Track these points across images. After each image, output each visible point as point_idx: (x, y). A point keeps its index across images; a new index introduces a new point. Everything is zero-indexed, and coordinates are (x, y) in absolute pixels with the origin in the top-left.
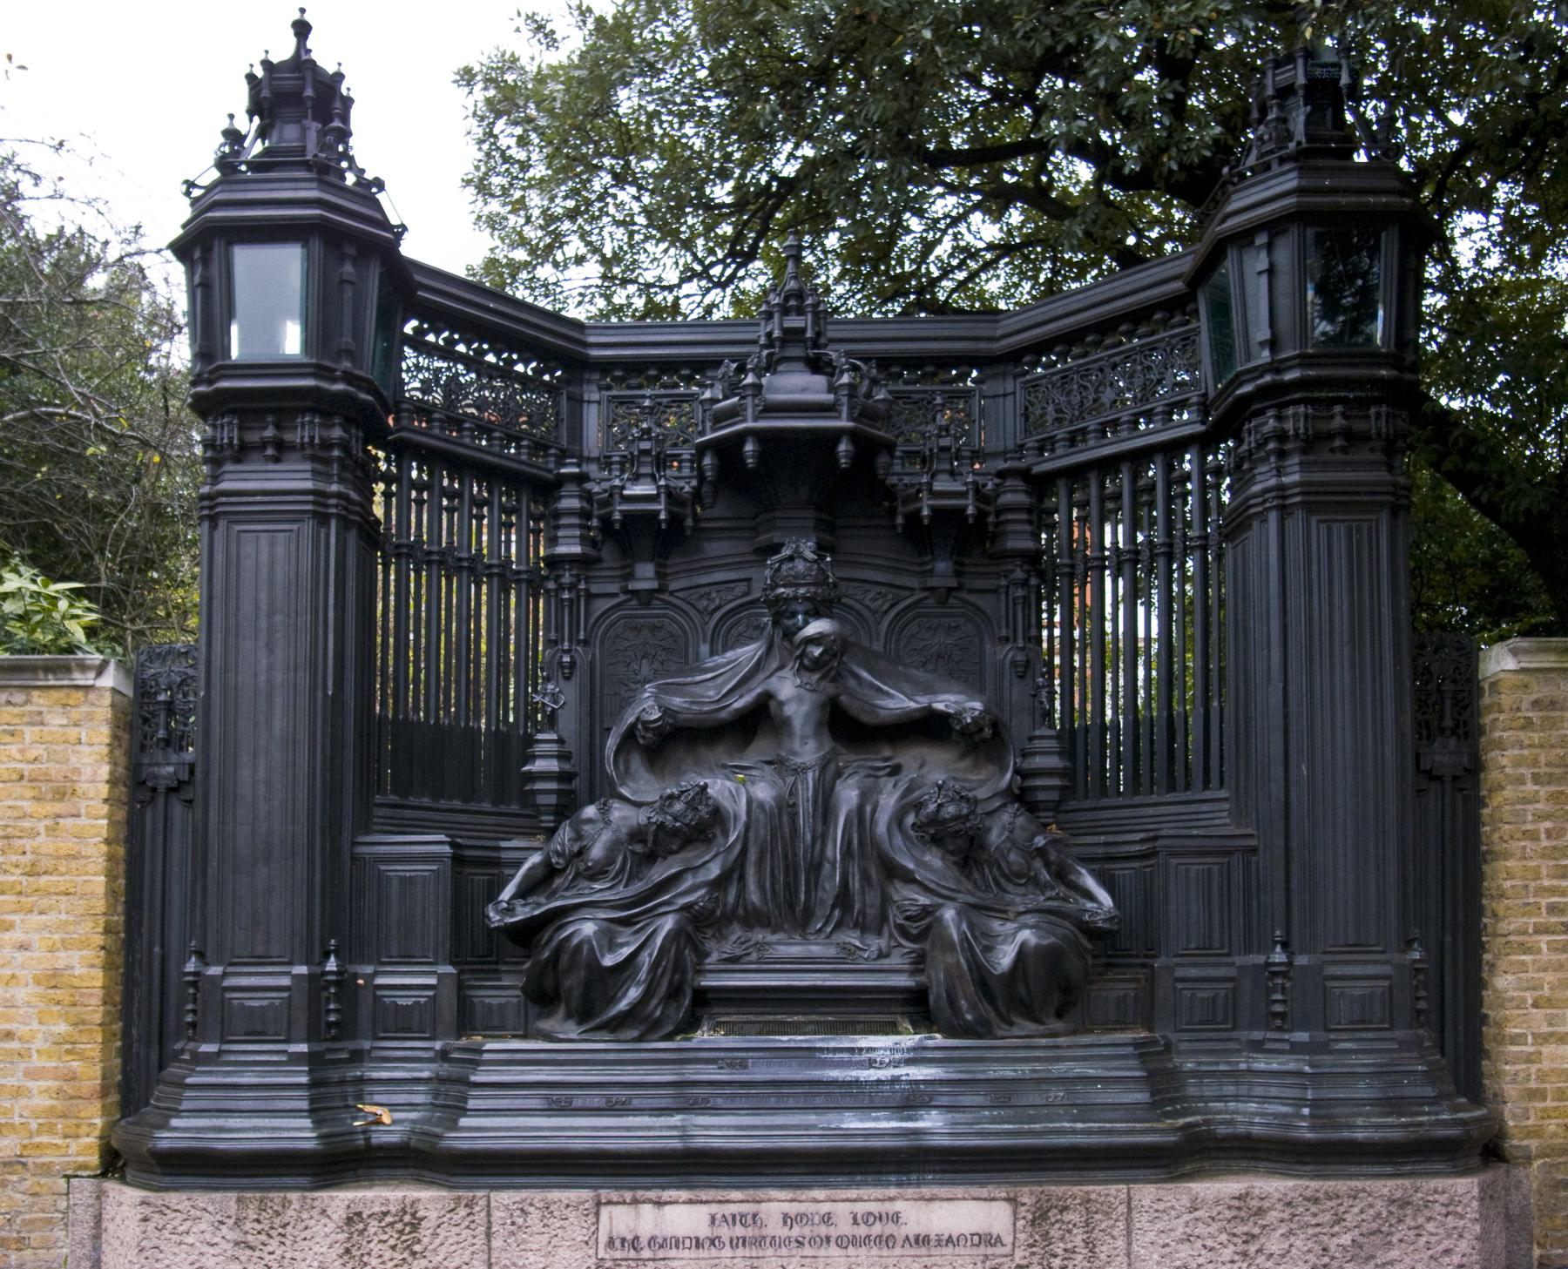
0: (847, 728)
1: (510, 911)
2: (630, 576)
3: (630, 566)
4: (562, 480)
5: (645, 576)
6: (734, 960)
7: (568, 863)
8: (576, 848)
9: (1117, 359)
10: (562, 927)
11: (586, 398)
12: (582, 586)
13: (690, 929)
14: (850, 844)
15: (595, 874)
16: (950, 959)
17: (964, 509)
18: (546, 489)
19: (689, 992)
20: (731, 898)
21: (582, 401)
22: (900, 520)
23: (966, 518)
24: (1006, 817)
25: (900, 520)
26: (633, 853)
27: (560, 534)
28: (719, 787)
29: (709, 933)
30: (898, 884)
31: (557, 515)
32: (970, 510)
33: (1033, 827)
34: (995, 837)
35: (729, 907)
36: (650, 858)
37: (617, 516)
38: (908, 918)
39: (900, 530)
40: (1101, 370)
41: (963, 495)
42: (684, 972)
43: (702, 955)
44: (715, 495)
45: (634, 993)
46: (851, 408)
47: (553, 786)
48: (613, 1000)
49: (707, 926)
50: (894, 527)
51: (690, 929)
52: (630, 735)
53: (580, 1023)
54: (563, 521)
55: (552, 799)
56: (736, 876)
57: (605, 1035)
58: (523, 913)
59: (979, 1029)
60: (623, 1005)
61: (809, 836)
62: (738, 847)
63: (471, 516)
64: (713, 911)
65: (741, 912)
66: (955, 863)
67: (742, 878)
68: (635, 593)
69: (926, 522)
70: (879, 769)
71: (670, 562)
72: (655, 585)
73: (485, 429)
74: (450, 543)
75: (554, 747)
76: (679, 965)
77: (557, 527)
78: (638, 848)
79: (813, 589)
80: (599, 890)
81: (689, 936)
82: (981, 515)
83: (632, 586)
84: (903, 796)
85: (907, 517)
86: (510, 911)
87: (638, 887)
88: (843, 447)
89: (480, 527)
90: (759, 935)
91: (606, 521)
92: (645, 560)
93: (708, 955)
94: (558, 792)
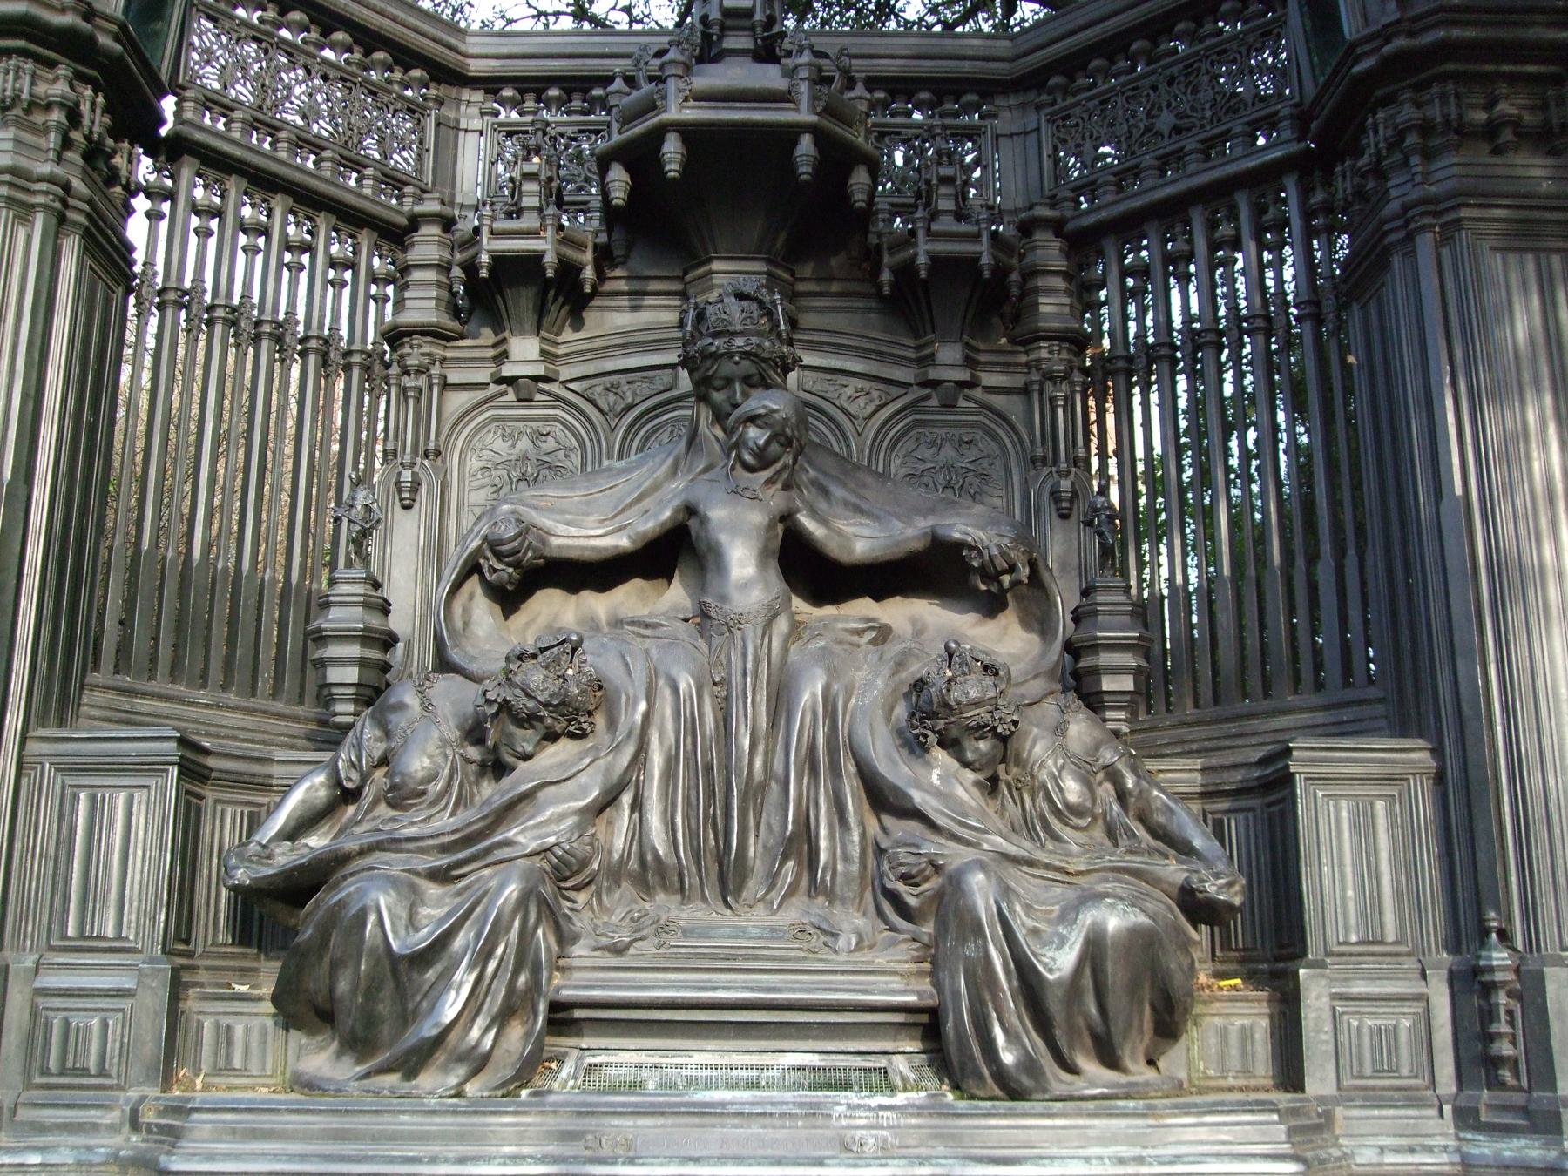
0: (809, 571)
1: (266, 853)
2: (502, 357)
3: (504, 340)
4: (415, 222)
5: (525, 352)
6: (618, 950)
7: (365, 778)
8: (377, 754)
9: (1175, 70)
10: (336, 886)
11: (463, 125)
12: (436, 370)
13: (547, 890)
14: (812, 748)
15: (400, 796)
16: (971, 950)
17: (974, 260)
18: (396, 235)
19: (542, 1007)
20: (619, 843)
21: (457, 129)
22: (886, 276)
23: (979, 272)
24: (1050, 709)
25: (886, 276)
26: (468, 761)
27: (407, 294)
28: (600, 659)
29: (582, 897)
30: (888, 820)
31: (405, 270)
32: (985, 260)
33: (1097, 733)
34: (1038, 748)
35: (616, 856)
36: (497, 768)
37: (485, 258)
38: (905, 878)
39: (886, 290)
40: (1154, 88)
41: (976, 237)
42: (536, 970)
43: (565, 938)
44: (629, 248)
45: (451, 1007)
46: (814, 98)
47: (354, 650)
48: (407, 1017)
49: (577, 888)
50: (879, 287)
51: (547, 890)
52: (472, 568)
53: (359, 1062)
54: (417, 275)
55: (352, 675)
56: (626, 799)
57: (393, 1079)
58: (284, 857)
59: (1026, 1081)
60: (429, 1030)
61: (747, 743)
62: (629, 751)
63: (281, 264)
64: (584, 863)
65: (633, 864)
66: (977, 784)
67: (638, 805)
68: (511, 381)
69: (923, 274)
70: (860, 632)
71: (561, 339)
72: (539, 370)
73: (306, 143)
74: (246, 296)
75: (359, 589)
76: (524, 955)
77: (406, 286)
78: (474, 753)
79: (754, 340)
80: (411, 825)
81: (543, 902)
82: (1001, 271)
83: (508, 371)
84: (895, 673)
85: (895, 271)
86: (266, 853)
87: (465, 816)
88: (806, 145)
89: (294, 283)
90: (663, 904)
91: (470, 268)
92: (522, 333)
93: (575, 938)
94: (363, 663)
